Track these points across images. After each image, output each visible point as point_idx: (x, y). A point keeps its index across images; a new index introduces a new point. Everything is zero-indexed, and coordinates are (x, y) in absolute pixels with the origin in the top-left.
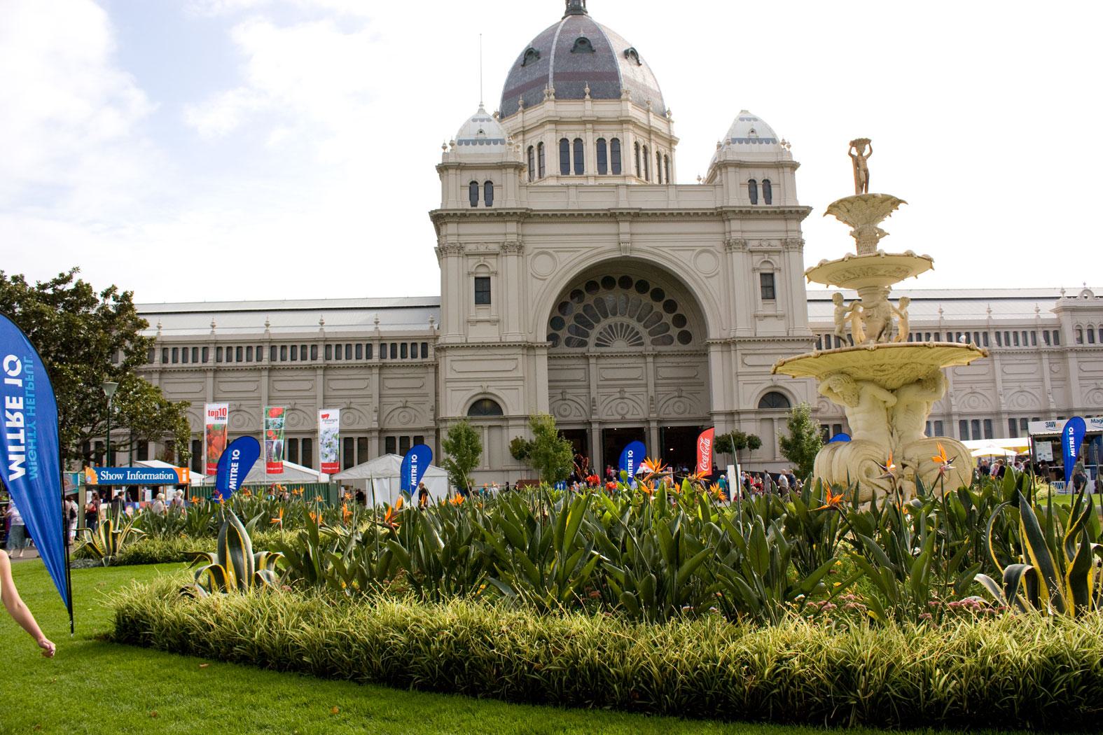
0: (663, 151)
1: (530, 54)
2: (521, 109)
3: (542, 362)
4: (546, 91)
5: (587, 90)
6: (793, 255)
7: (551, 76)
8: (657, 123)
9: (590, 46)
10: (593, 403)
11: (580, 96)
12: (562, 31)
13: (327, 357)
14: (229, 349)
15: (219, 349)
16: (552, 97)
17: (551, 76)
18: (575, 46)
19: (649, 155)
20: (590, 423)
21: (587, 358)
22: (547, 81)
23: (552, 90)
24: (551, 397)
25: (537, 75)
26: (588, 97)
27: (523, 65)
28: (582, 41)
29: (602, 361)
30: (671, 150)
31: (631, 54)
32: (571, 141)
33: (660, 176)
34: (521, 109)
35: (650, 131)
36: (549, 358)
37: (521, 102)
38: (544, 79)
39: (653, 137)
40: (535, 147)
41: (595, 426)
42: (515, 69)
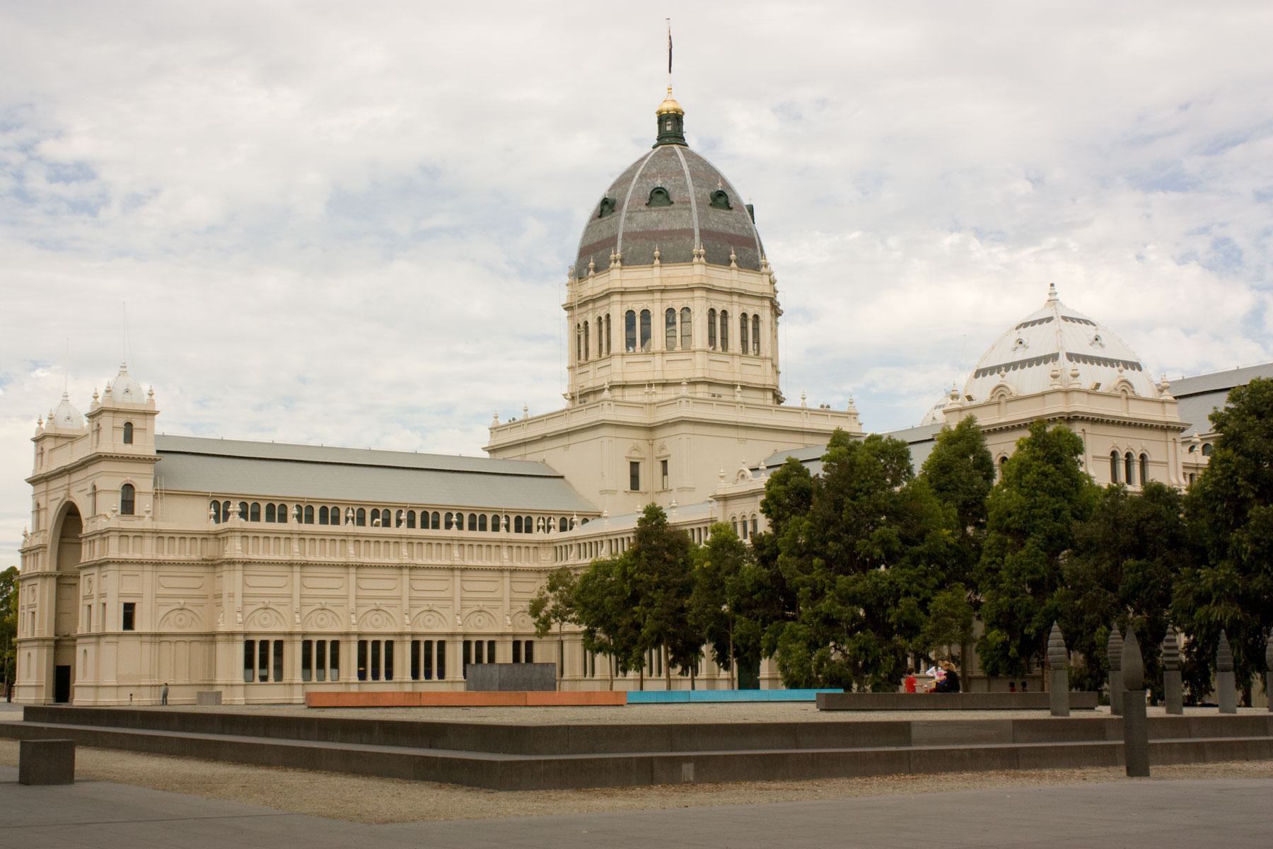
1: (607, 206)
2: (592, 273)
4: (612, 256)
5: (657, 253)
7: (620, 236)
9: (668, 197)
11: (649, 262)
12: (642, 176)
16: (619, 264)
17: (620, 236)
18: (651, 198)
19: (730, 321)
22: (615, 244)
23: (619, 255)
25: (606, 234)
26: (657, 262)
27: (600, 217)
28: (659, 191)
32: (638, 314)
33: (744, 342)
34: (592, 273)
37: (592, 264)
38: (612, 241)
39: (735, 298)
40: (603, 318)
42: (593, 219)
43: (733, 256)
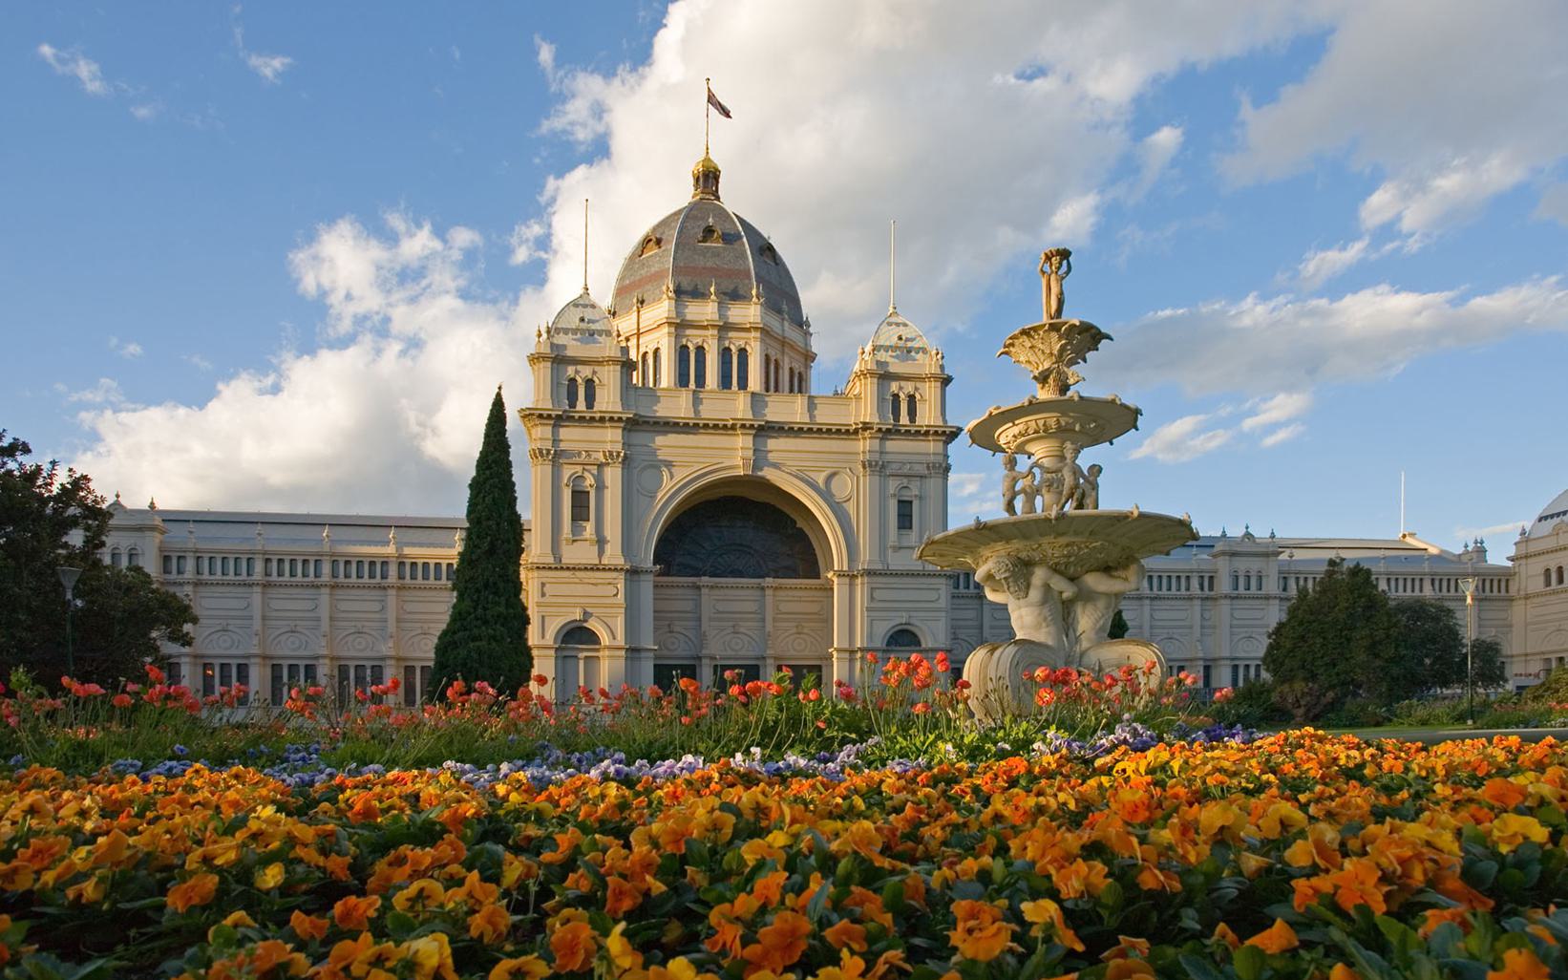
0: (798, 367)
3: (647, 585)
6: (933, 484)
8: (792, 333)
10: (702, 637)
13: (401, 577)
14: (280, 561)
15: (268, 561)
20: (700, 658)
21: (699, 588)
24: (656, 629)
29: (716, 592)
30: (808, 367)
31: (766, 251)
35: (783, 343)
36: (656, 586)
41: (705, 661)
43: (785, 307)
